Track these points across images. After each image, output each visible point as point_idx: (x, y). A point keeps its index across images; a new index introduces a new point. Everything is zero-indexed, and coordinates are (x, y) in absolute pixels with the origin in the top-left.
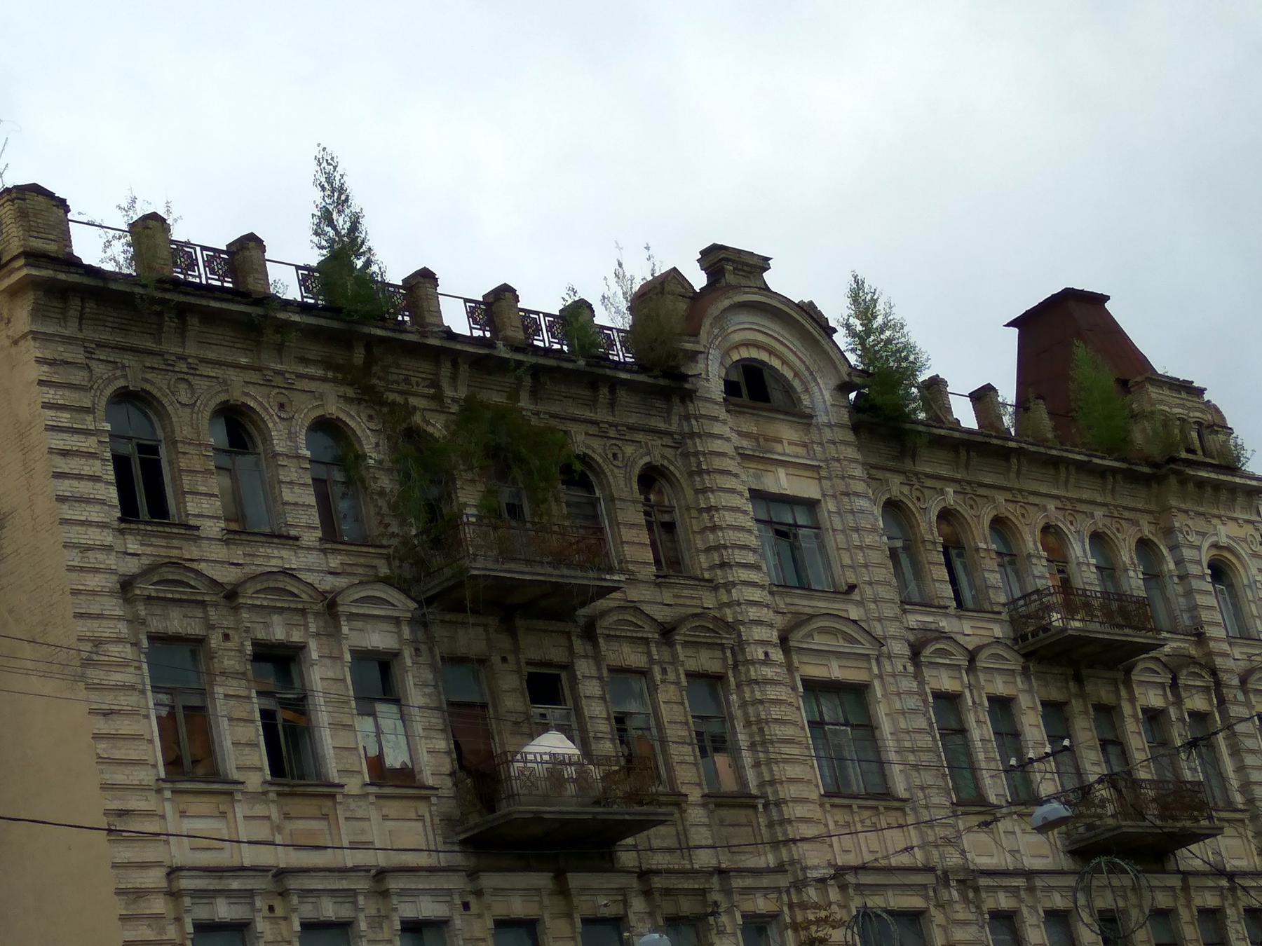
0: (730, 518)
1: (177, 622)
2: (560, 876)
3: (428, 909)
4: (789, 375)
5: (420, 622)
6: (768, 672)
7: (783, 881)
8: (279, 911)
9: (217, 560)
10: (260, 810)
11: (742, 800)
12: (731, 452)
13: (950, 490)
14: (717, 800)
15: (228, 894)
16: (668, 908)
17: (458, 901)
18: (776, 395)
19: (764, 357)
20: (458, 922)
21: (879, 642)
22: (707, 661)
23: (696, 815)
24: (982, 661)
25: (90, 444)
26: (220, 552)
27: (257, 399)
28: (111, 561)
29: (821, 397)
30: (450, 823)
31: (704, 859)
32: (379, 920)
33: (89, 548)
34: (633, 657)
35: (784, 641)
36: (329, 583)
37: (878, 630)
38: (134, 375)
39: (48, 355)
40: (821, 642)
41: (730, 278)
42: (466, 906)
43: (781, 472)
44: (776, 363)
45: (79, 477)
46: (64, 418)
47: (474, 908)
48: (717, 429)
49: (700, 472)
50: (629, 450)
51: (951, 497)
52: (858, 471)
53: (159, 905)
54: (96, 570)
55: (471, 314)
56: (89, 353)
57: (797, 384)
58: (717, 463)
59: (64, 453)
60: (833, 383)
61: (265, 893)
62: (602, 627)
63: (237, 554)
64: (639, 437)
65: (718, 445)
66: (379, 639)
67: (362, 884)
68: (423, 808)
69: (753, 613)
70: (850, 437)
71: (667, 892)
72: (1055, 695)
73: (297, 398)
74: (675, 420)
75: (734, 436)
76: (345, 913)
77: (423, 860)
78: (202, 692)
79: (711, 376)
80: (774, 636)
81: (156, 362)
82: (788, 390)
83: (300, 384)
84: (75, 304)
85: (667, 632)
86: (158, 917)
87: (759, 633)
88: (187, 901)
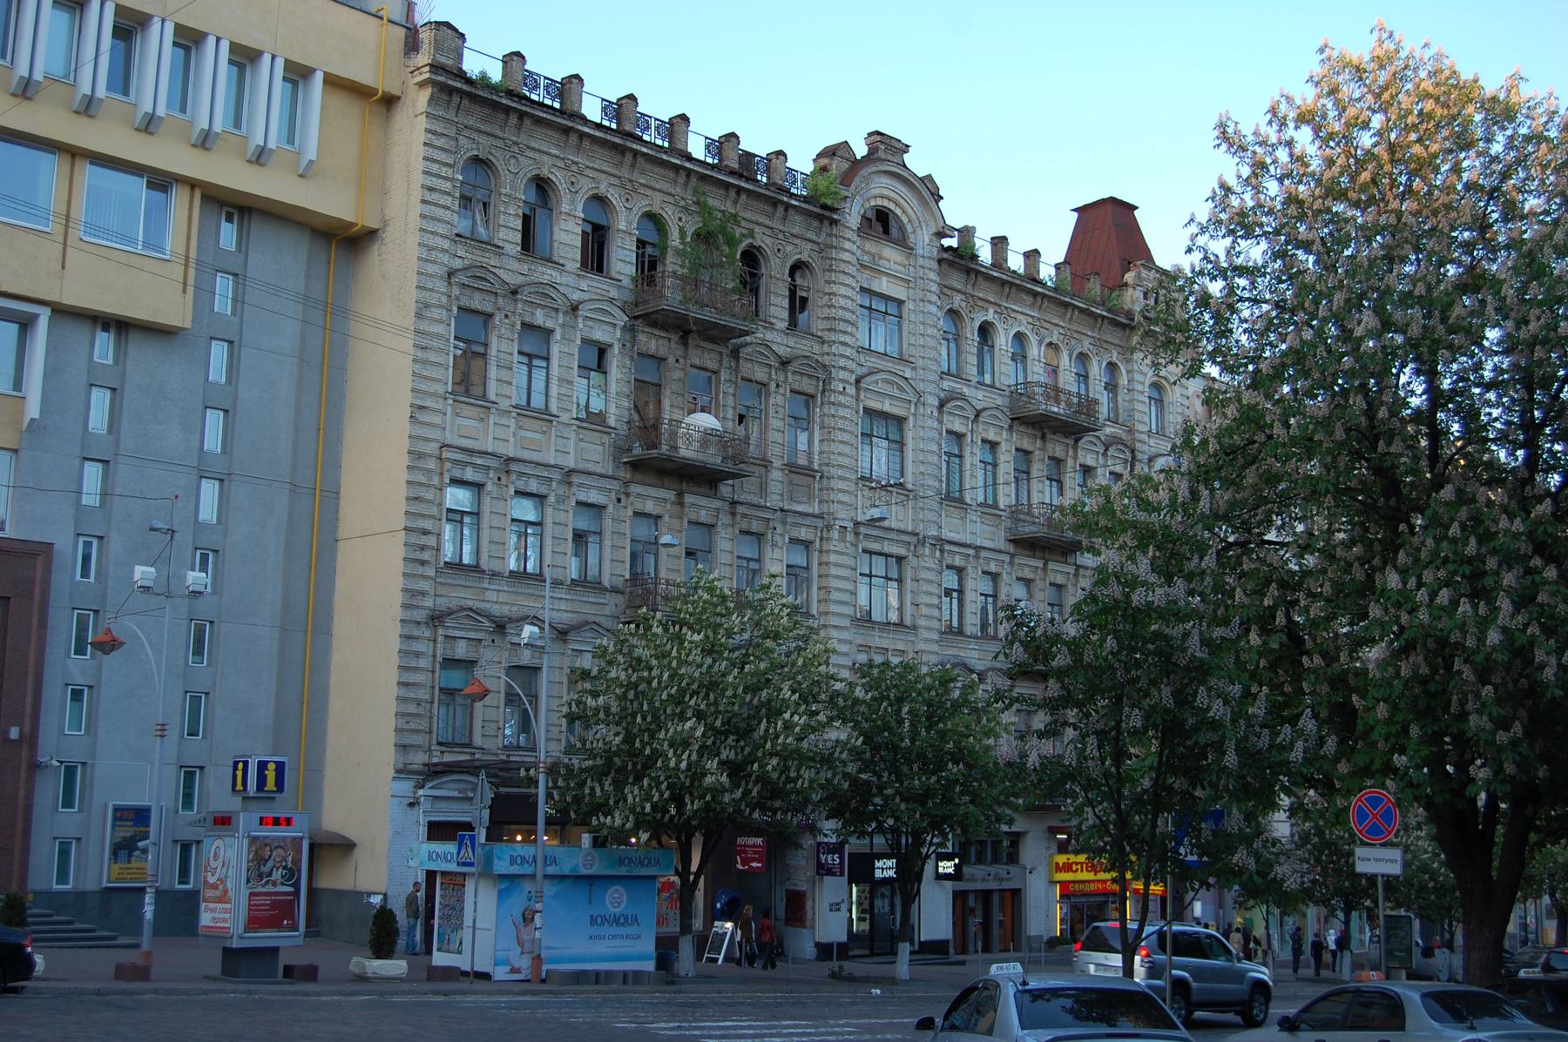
0: (842, 302)
1: (477, 302)
2: (680, 495)
3: (594, 497)
4: (905, 220)
5: (630, 329)
6: (842, 399)
7: (820, 523)
8: (504, 481)
9: (512, 269)
10: (504, 421)
11: (808, 472)
12: (854, 261)
13: (991, 311)
14: (792, 468)
15: (475, 466)
16: (745, 526)
17: (613, 495)
18: (894, 232)
19: (892, 206)
20: (610, 509)
21: (919, 394)
22: (807, 385)
23: (776, 475)
24: (984, 417)
25: (447, 186)
26: (515, 265)
27: (559, 178)
28: (446, 259)
29: (922, 239)
30: (619, 450)
31: (773, 501)
32: (561, 500)
33: (434, 249)
34: (760, 374)
35: (858, 381)
36: (576, 296)
37: (921, 387)
38: (483, 146)
39: (433, 127)
40: (881, 387)
41: (881, 154)
42: (619, 500)
43: (884, 279)
44: (898, 212)
45: (436, 205)
46: (435, 168)
47: (623, 502)
48: (847, 245)
49: (830, 270)
50: (789, 248)
51: (990, 316)
52: (934, 288)
53: (432, 464)
54: (435, 262)
55: (707, 147)
56: (459, 132)
57: (909, 228)
58: (842, 266)
59: (431, 189)
60: (934, 230)
61: (496, 470)
62: (744, 352)
63: (524, 268)
64: (797, 241)
65: (846, 256)
66: (600, 335)
67: (557, 476)
68: (606, 439)
69: (842, 362)
70: (935, 265)
71: (744, 516)
72: (1026, 445)
73: (583, 180)
74: (823, 235)
75: (859, 253)
76: (543, 490)
77: (599, 470)
78: (486, 345)
79: (852, 217)
80: (852, 380)
81: (500, 143)
82: (902, 229)
83: (587, 172)
84: (456, 99)
85: (784, 363)
86: (430, 471)
87: (842, 375)
88: (448, 465)
